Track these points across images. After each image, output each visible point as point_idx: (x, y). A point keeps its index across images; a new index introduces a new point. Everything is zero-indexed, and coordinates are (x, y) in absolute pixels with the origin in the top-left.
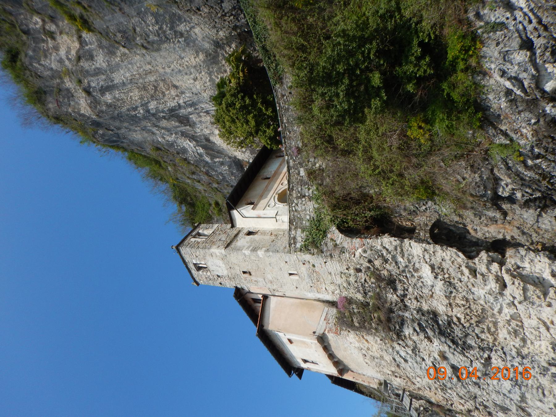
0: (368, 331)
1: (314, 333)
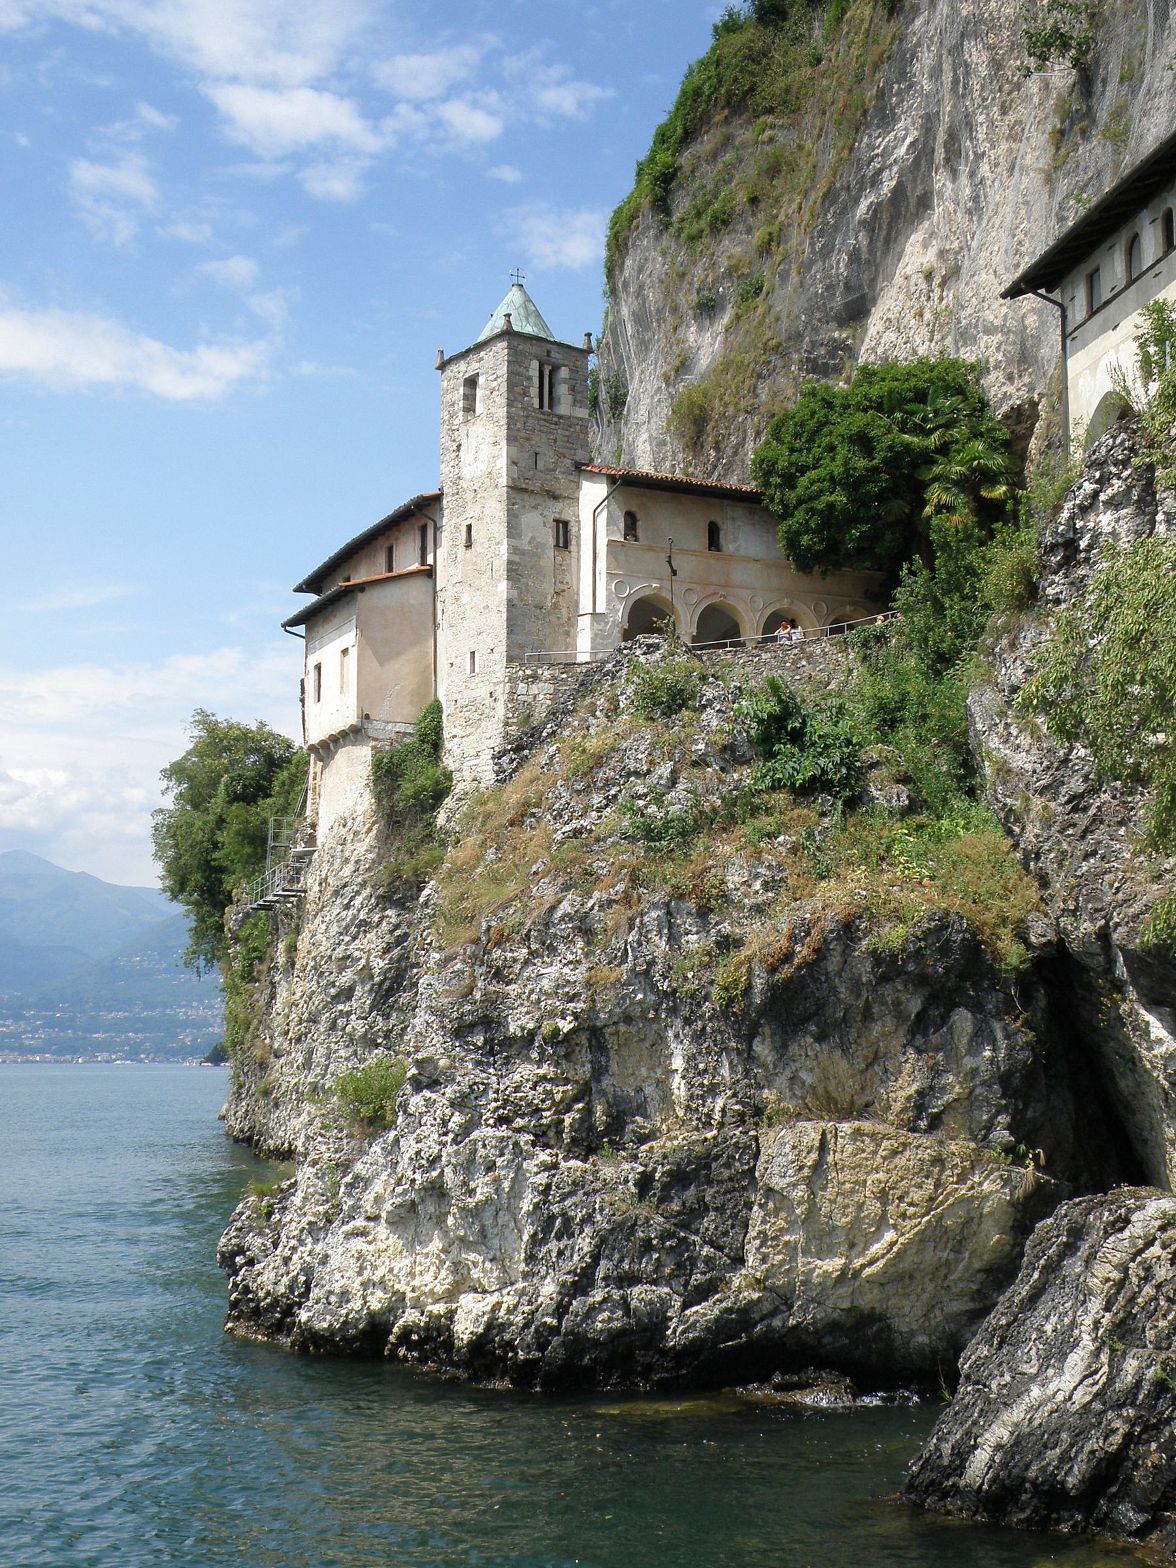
1: (367, 717)
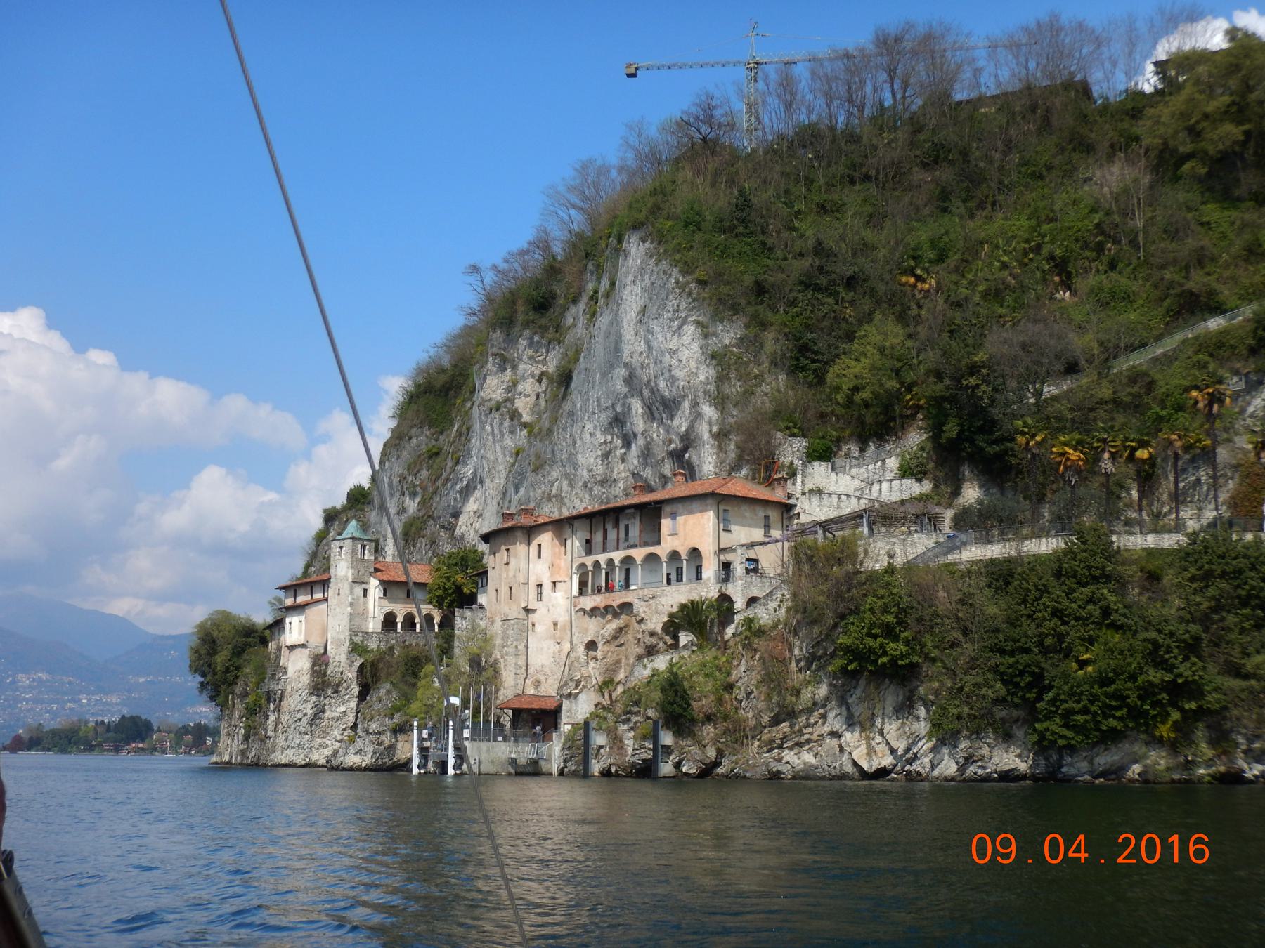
0: (312, 675)
